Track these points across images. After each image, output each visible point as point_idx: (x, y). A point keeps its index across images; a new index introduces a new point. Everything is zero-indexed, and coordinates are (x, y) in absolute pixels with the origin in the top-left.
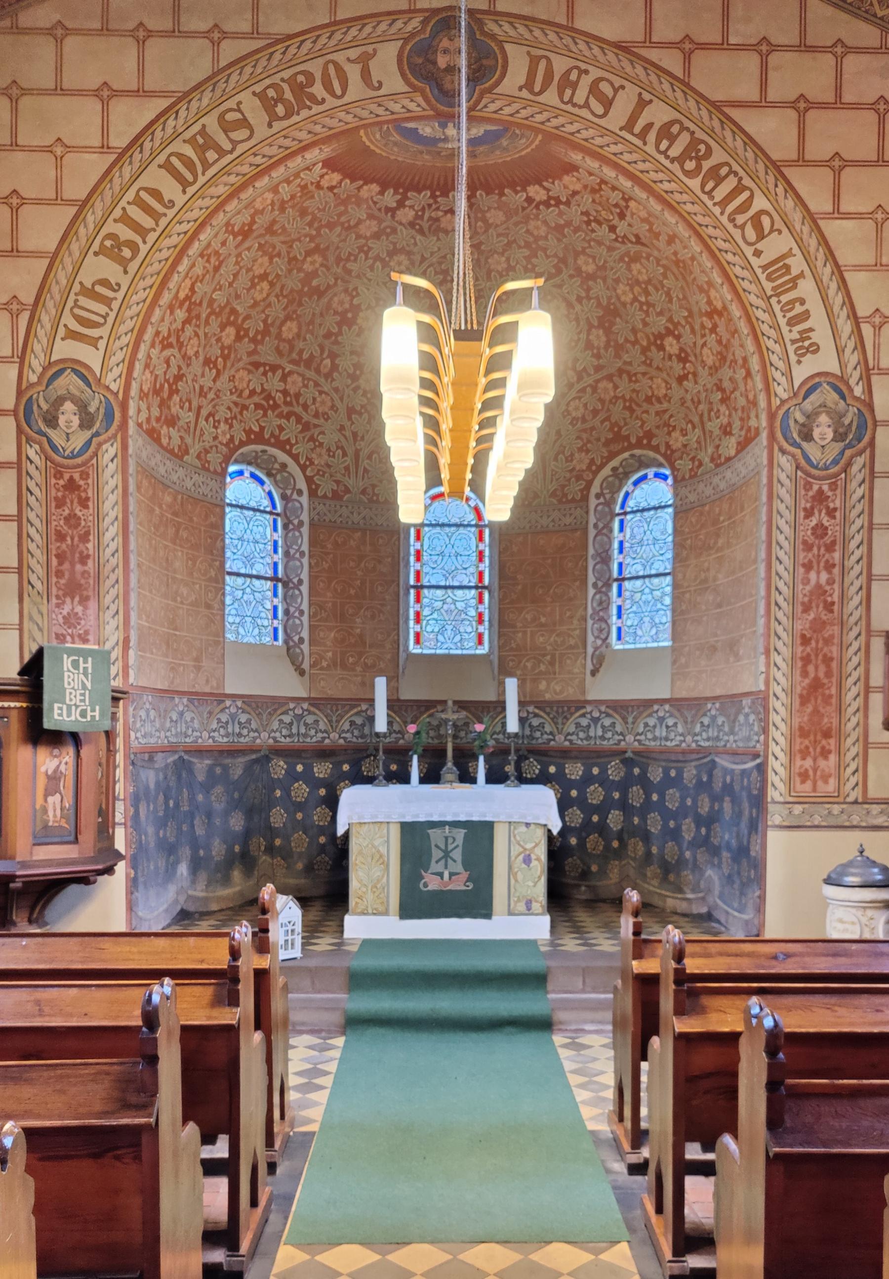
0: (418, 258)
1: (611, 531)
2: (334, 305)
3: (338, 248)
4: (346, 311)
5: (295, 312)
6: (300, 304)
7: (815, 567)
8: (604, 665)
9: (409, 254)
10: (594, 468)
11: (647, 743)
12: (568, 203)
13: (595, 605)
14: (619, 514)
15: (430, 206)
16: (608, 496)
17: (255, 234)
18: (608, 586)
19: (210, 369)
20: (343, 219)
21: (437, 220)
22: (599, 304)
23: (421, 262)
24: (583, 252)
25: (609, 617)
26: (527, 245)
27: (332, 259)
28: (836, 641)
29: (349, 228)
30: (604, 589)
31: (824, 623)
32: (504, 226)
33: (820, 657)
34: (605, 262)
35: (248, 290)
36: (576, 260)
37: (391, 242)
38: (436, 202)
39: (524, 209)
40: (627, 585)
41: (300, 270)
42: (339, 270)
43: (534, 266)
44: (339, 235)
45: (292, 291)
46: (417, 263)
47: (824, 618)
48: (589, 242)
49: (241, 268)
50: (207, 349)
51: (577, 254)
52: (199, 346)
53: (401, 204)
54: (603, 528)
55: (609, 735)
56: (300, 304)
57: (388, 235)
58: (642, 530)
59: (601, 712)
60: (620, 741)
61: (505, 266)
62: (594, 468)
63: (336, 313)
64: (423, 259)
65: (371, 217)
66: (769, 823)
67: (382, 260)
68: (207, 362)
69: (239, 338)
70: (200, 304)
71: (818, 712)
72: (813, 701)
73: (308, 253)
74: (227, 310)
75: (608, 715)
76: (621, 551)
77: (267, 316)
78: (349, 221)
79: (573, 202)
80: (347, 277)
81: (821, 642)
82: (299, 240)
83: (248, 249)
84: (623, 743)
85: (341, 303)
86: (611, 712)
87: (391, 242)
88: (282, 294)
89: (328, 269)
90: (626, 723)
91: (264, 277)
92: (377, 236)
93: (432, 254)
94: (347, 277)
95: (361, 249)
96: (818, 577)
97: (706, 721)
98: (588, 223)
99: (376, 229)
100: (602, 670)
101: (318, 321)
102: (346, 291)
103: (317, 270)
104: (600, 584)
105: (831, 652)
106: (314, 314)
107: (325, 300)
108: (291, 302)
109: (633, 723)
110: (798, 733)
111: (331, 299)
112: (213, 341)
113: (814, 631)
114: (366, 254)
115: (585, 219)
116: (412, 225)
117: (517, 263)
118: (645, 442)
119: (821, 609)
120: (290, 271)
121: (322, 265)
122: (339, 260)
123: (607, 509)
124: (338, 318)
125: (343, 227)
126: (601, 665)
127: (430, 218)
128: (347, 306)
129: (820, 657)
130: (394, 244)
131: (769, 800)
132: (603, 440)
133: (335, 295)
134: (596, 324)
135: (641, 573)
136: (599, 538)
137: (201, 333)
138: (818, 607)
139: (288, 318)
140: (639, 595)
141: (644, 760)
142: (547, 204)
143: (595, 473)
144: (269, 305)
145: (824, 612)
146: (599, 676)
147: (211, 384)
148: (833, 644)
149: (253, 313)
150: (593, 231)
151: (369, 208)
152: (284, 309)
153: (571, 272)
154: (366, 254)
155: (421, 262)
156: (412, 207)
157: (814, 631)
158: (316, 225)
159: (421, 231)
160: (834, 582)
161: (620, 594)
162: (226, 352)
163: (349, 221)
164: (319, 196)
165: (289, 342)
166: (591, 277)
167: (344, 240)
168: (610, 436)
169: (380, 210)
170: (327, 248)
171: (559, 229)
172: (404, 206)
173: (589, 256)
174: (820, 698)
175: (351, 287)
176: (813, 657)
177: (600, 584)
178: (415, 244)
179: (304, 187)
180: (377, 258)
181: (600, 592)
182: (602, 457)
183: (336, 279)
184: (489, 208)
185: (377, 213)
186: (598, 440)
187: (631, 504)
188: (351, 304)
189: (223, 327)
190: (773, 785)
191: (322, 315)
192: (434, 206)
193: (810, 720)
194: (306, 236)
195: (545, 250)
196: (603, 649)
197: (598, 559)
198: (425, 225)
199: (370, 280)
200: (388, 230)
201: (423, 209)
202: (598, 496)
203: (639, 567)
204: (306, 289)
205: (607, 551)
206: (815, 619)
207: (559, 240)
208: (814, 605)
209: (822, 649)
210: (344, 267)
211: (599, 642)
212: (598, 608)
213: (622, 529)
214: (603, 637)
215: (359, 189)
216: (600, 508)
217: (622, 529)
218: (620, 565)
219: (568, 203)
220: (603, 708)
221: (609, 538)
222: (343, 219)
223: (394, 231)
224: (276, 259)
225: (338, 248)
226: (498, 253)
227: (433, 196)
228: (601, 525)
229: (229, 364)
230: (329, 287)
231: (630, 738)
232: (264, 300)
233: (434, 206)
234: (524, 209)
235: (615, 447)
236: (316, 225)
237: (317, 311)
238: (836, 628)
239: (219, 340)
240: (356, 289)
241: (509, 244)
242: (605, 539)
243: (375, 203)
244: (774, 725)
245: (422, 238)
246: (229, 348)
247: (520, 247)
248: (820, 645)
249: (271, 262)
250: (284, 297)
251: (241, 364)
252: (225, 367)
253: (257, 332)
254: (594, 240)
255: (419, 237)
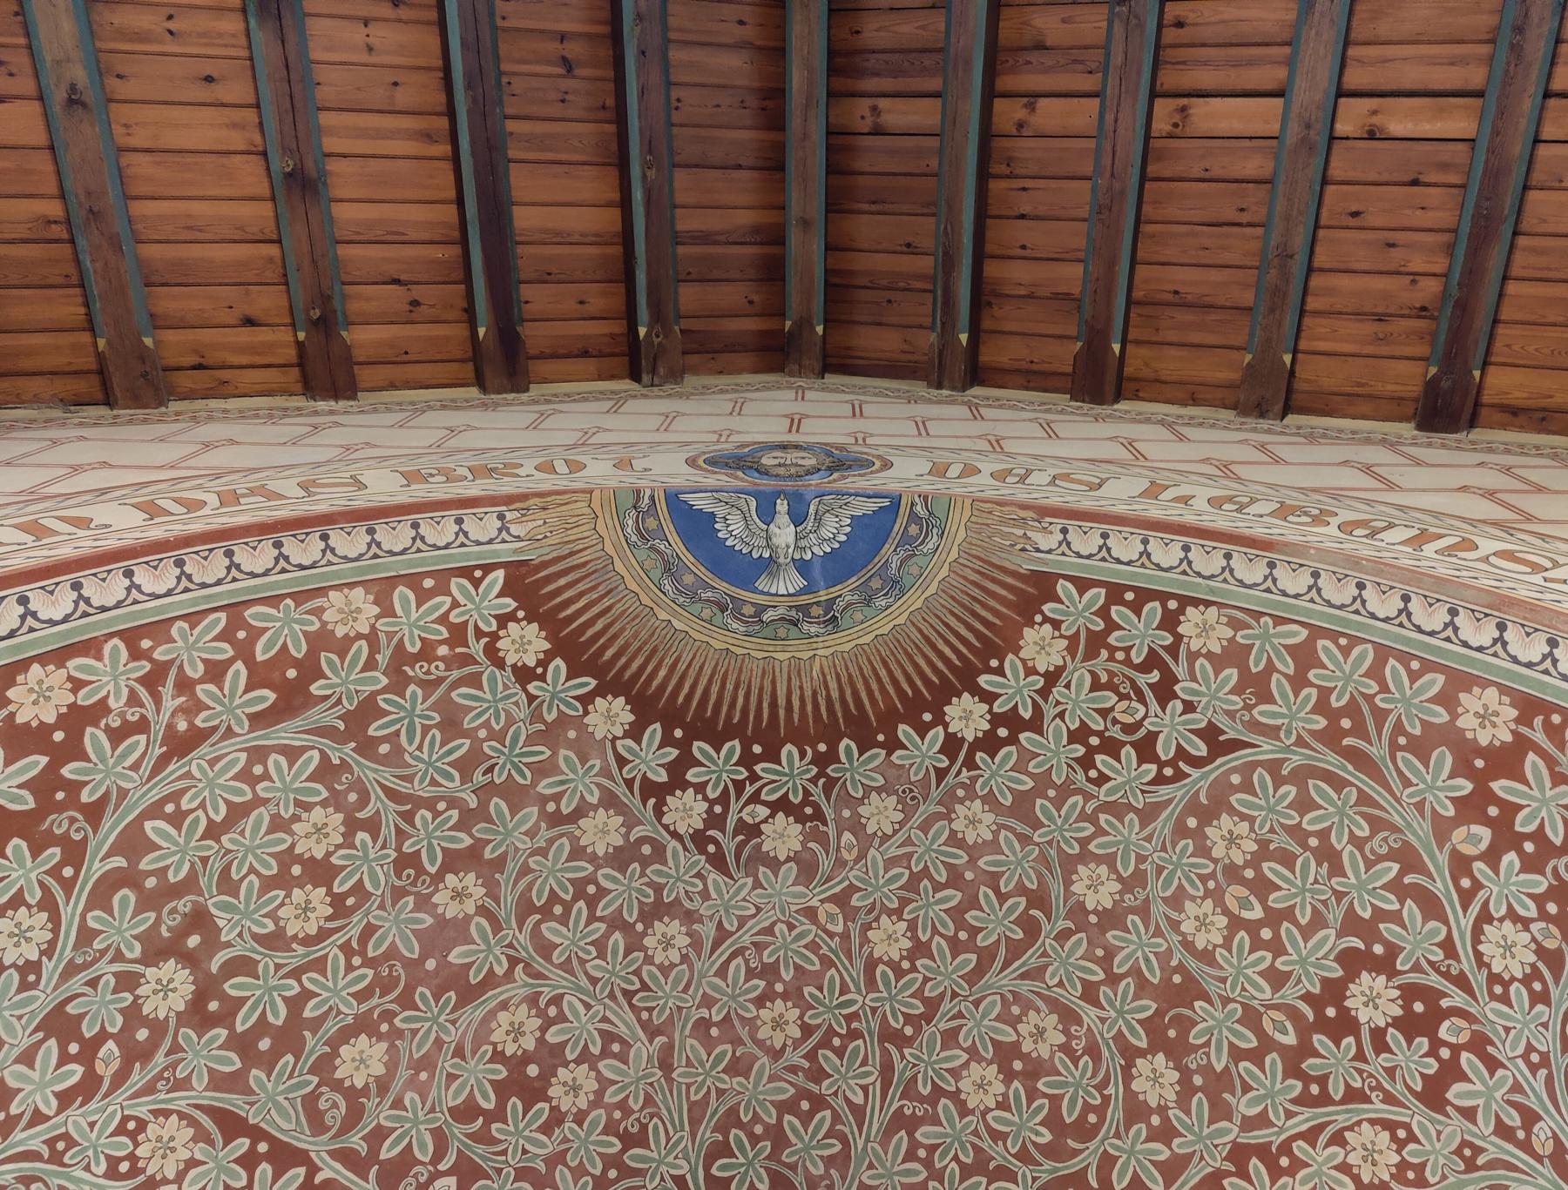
0: (708, 931)
2: (497, 1036)
3: (525, 870)
4: (526, 1059)
5: (388, 1016)
6: (407, 1001)
9: (690, 917)
12: (1036, 724)
15: (739, 786)
17: (317, 715)
19: (64, 1059)
20: (544, 787)
21: (754, 831)
22: (1143, 985)
23: (717, 944)
24: (1085, 857)
26: (955, 879)
27: (509, 898)
29: (556, 819)
32: (901, 837)
34: (1141, 859)
35: (268, 884)
36: (1068, 883)
37: (651, 884)
38: (754, 778)
39: (941, 774)
41: (423, 903)
42: (523, 938)
43: (974, 931)
44: (532, 834)
45: (392, 953)
46: (708, 946)
48: (1092, 819)
49: (258, 802)
50: (76, 983)
51: (1069, 865)
52: (49, 951)
53: (677, 781)
56: (407, 1001)
57: (645, 862)
61: (907, 944)
63: (498, 1056)
64: (722, 935)
65: (610, 801)
67: (626, 928)
68: (59, 1024)
69: (197, 1015)
70: (94, 813)
73: (454, 862)
74: (184, 905)
77: (307, 995)
78: (557, 798)
79: (1049, 711)
80: (539, 964)
82: (430, 805)
83: (292, 753)
85: (517, 1032)
87: (651, 884)
88: (362, 952)
89: (497, 927)
91: (320, 872)
92: (621, 858)
93: (742, 921)
94: (539, 964)
95: (579, 886)
98: (1086, 762)
99: (620, 842)
101: (447, 1064)
102: (533, 1001)
103: (468, 919)
106: (439, 1043)
107: (473, 1014)
108: (385, 986)
111: (492, 1014)
112: (107, 970)
114: (592, 903)
115: (1080, 750)
116: (700, 840)
117: (935, 931)
120: (398, 894)
121: (482, 910)
122: (525, 908)
124: (502, 1073)
125: (542, 812)
127: (741, 827)
128: (529, 1043)
130: (658, 889)
133: (504, 1006)
134: (1143, 1044)
137: (70, 912)
139: (363, 1026)
142: (989, 744)
144: (319, 965)
147: (50, 1107)
149: (266, 962)
150: (1102, 779)
151: (605, 772)
152: (361, 996)
153: (1062, 924)
154: (592, 903)
155: (717, 944)
156: (700, 788)
158: (479, 778)
159: (718, 861)
162: (142, 1034)
163: (557, 798)
164: (492, 679)
165: (354, 1095)
166: (1112, 918)
167: (543, 852)
169: (629, 783)
170: (500, 863)
171: (1022, 807)
172: (685, 785)
173: (1099, 860)
175: (547, 993)
178: (705, 895)
179: (458, 634)
180: (616, 922)
183: (513, 962)
184: (868, 790)
185: (621, 791)
188: (541, 1041)
189: (155, 952)
191: (459, 1052)
192: (749, 790)
194: (453, 803)
195: (993, 880)
198: (729, 845)
199: (594, 981)
200: (646, 850)
201: (724, 799)
204: (431, 964)
207: (1024, 840)
210: (536, 932)
215: (586, 700)
219: (1036, 724)
222: (544, 787)
223: (659, 853)
224: (362, 836)
225: (525, 870)
226: (889, 913)
227: (747, 760)
229: (137, 1078)
230: (490, 981)
232: (308, 941)
233: (749, 790)
234: (941, 774)
236: (479, 778)
237: (451, 1037)
239: (128, 982)
240: (557, 1000)
241: (912, 884)
243: (622, 762)
245: (720, 879)
246: (158, 1028)
247: (938, 887)
249: (349, 835)
250: (368, 963)
251: (181, 1101)
252: (120, 1078)
253: (262, 1026)
254: (1107, 807)
255: (713, 876)
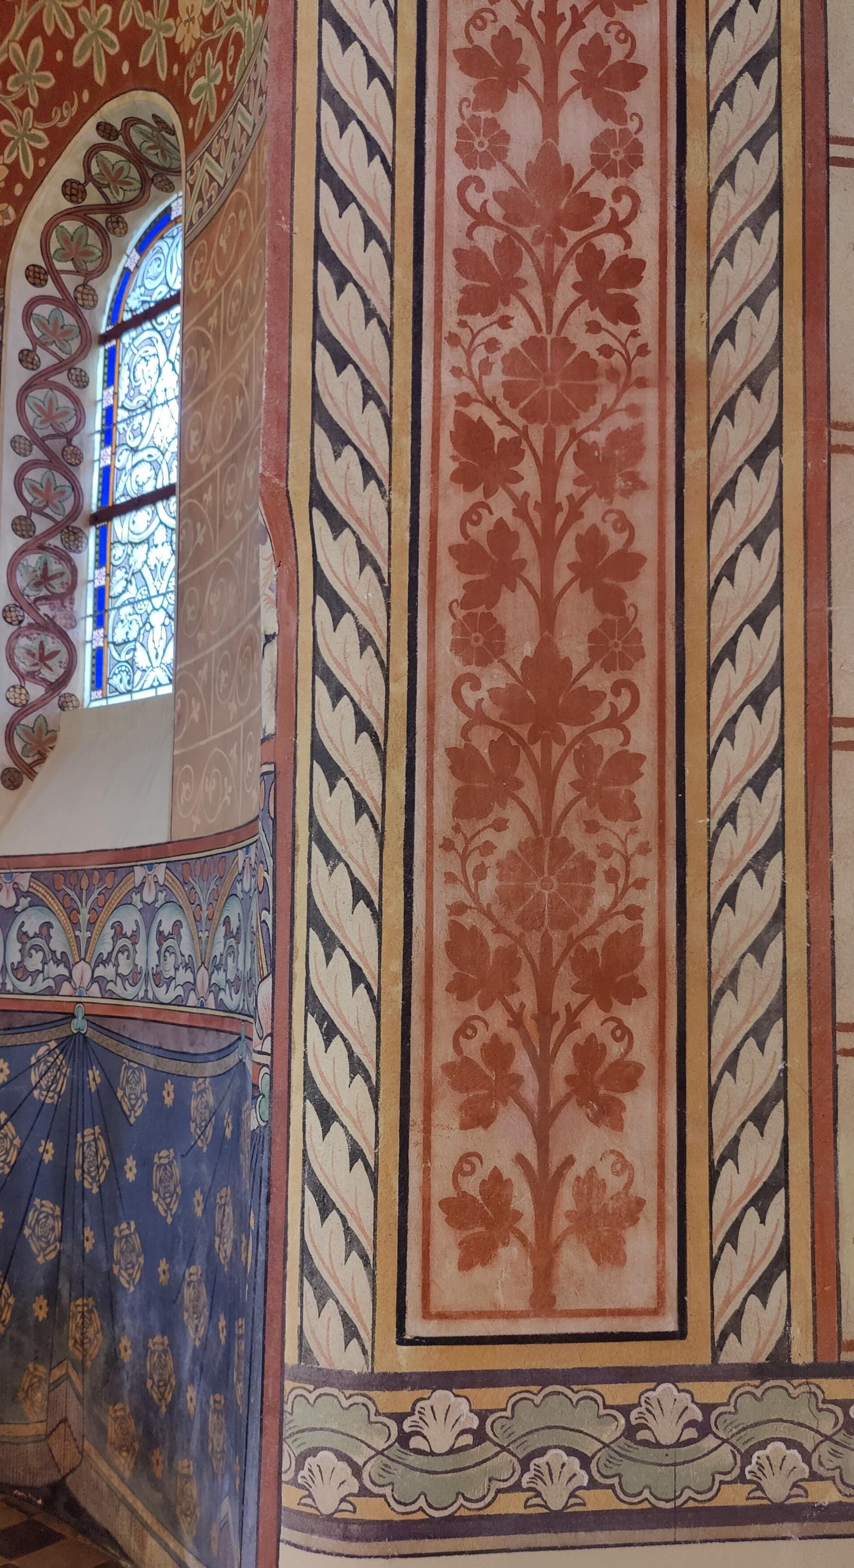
1: (83, 381)
7: (536, 77)
8: (51, 756)
10: (18, 190)
11: (119, 990)
13: (21, 581)
14: (104, 339)
16: (71, 282)
18: (75, 537)
25: (73, 622)
28: (648, 468)
30: (55, 542)
31: (585, 360)
33: (568, 552)
40: (120, 527)
47: (588, 343)
54: (55, 369)
55: (34, 962)
58: (154, 362)
59: (20, 894)
60: (60, 980)
62: (18, 190)
66: (290, 1497)
71: (562, 849)
72: (529, 793)
75: (36, 903)
76: (108, 437)
81: (569, 468)
84: (66, 988)
86: (41, 891)
90: (75, 925)
96: (551, 129)
97: (129, 919)
100: (42, 771)
104: (41, 525)
105: (625, 525)
109: (91, 924)
110: (444, 970)
113: (532, 414)
118: (125, 68)
119: (565, 294)
123: (69, 319)
126: (42, 758)
129: (568, 552)
131: (291, 1356)
132: (34, 101)
135: (149, 488)
136: (39, 394)
138: (549, 284)
140: (141, 551)
141: (109, 1043)
143: (21, 204)
145: (584, 313)
146: (31, 789)
148: (637, 483)
157: (532, 414)
160: (635, 159)
161: (102, 559)
168: (49, 82)
174: (568, 773)
176: (527, 549)
177: (41, 525)
181: (42, 548)
182: (37, 154)
186: (22, 103)
187: (134, 302)
190: (308, 1269)
193: (507, 899)
196: (51, 710)
197: (37, 453)
202: (35, 275)
203: (144, 473)
205: (68, 436)
206: (534, 345)
208: (527, 270)
209: (576, 514)
211: (36, 691)
212: (32, 594)
213: (110, 379)
214: (52, 677)
216: (43, 310)
217: (110, 379)
218: (106, 473)
220: (24, 881)
221: (76, 401)
228: (46, 360)
231: (82, 972)
235: (61, 117)
238: (649, 398)
242: (63, 401)
244: (315, 921)
248: (565, 488)
